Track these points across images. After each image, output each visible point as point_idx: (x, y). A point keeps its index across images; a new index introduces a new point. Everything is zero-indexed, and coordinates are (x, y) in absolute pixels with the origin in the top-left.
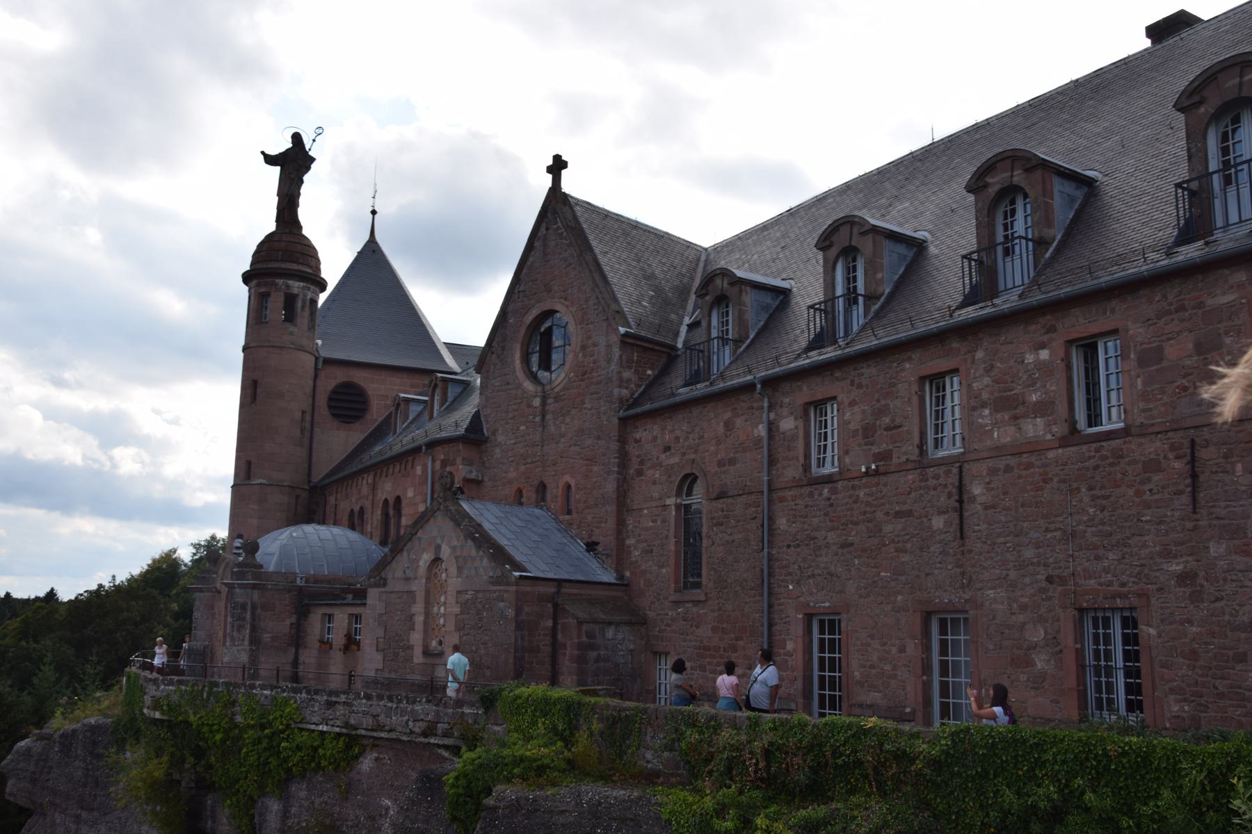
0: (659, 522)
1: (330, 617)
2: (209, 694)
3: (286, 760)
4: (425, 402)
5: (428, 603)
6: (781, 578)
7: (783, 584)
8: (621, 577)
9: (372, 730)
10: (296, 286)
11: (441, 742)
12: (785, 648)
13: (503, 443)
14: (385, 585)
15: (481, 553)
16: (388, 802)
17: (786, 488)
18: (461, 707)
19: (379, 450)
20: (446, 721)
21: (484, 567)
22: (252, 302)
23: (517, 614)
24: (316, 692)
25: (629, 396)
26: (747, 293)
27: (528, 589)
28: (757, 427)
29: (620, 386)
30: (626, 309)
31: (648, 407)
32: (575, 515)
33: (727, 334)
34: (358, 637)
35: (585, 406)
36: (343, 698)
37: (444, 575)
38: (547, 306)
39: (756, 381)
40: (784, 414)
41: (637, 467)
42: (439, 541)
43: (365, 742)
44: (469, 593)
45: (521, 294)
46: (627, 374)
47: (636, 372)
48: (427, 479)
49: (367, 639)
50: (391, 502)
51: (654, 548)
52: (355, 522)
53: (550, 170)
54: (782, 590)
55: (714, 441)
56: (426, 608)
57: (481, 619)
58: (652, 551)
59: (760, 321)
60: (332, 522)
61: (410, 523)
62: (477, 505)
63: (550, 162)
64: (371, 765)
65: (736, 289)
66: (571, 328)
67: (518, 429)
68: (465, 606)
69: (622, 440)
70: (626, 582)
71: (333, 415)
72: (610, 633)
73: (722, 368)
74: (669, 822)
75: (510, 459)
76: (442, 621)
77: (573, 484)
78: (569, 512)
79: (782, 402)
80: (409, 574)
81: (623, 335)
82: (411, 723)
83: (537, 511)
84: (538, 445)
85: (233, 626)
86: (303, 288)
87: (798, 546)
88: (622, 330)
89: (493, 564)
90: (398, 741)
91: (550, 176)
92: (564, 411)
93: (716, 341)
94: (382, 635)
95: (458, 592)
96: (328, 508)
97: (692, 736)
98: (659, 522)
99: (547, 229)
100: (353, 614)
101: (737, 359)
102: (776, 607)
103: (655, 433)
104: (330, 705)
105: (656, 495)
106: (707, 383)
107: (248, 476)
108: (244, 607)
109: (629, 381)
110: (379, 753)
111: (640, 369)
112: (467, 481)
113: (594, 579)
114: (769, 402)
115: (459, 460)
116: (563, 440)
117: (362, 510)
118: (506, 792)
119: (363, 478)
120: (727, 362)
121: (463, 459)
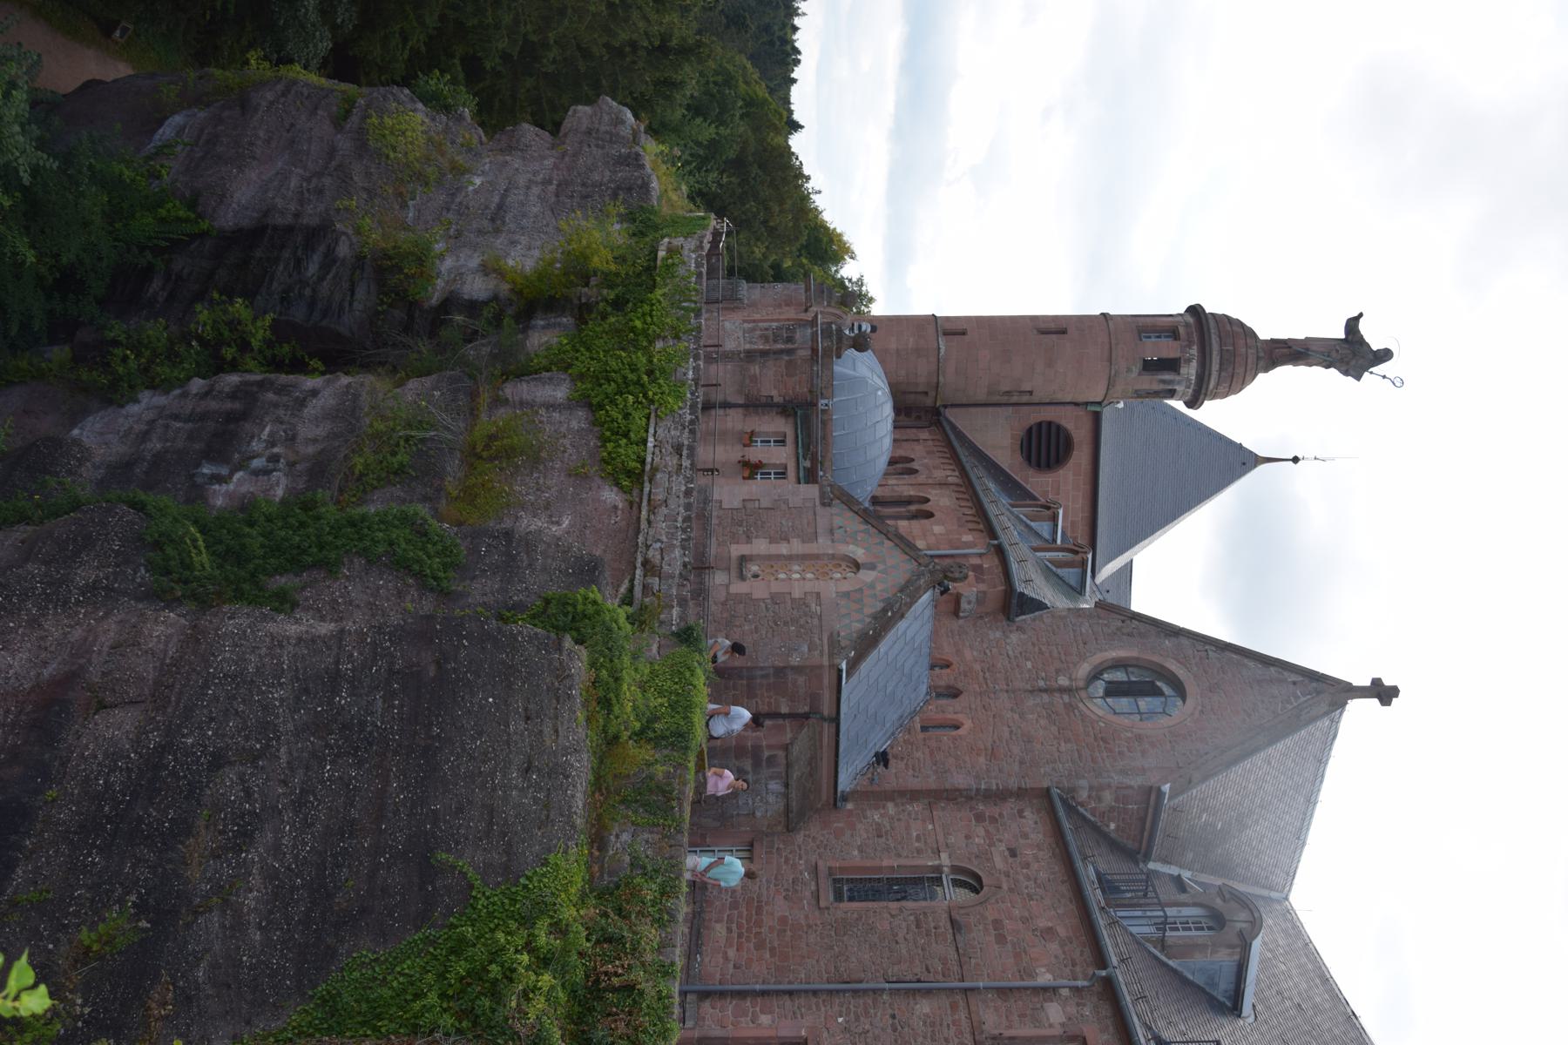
0: (917, 844)
1: (781, 442)
2: (686, 309)
3: (613, 402)
4: (1054, 540)
5: (803, 558)
6: (851, 1007)
7: (844, 1009)
8: (845, 799)
9: (649, 500)
10: (1190, 371)
11: (636, 582)
12: (762, 1012)
13: (1008, 641)
14: (823, 504)
15: (868, 620)
16: (566, 523)
17: (970, 1014)
18: (680, 604)
19: (989, 489)
20: (662, 587)
21: (851, 624)
22: (1165, 319)
23: (793, 668)
24: (692, 432)
25: (1080, 800)
26: (1231, 955)
27: (826, 681)
28: (1048, 971)
29: (1091, 788)
30: (1194, 791)
31: (1067, 825)
32: (921, 736)
33: (1172, 929)
34: (759, 476)
35: (1063, 744)
36: (686, 463)
37: (839, 575)
38: (1191, 688)
39: (1110, 970)
40: (1069, 1009)
41: (987, 814)
42: (881, 567)
43: (635, 492)
44: (818, 608)
45: (1204, 654)
46: (1108, 797)
47: (1112, 809)
48: (957, 548)
49: (757, 488)
50: (926, 507)
51: (883, 840)
52: (899, 465)
53: (1377, 682)
54: (836, 1008)
55: (1026, 914)
56: (797, 556)
57: (786, 623)
58: (880, 836)
59: (1193, 974)
60: (897, 437)
61: (901, 531)
62: (928, 612)
63: (1387, 682)
64: (609, 500)
65: (1236, 941)
66: (1164, 721)
67: (1027, 659)
68: (801, 604)
69: (1020, 793)
70: (839, 804)
71: (1030, 431)
72: (775, 786)
73: (1125, 923)
74: (545, 863)
75: (988, 651)
76: (782, 576)
77: (961, 732)
78: (924, 729)
79: (1084, 1005)
80: (838, 534)
81: (1159, 790)
82: (658, 545)
83: (924, 688)
84: (1008, 685)
85: (766, 329)
86: (1189, 380)
87: (895, 1030)
88: (1166, 788)
89: (855, 635)
90: (638, 531)
91: (1368, 683)
92: (1053, 716)
93: (1161, 913)
94: (762, 506)
95: (818, 594)
96: (914, 430)
97: (649, 891)
98: (917, 844)
99: (1294, 683)
100: (786, 468)
101: (1138, 943)
102: (814, 1000)
103: (1032, 836)
104: (678, 449)
105: (952, 839)
106: (1103, 904)
107: (946, 334)
108: (790, 340)
109: (1099, 799)
110: (622, 510)
111: (1116, 814)
112: (957, 599)
113: (841, 764)
114: (1083, 987)
115: (983, 587)
116: (1016, 716)
117: (916, 471)
118: (579, 662)
119: (954, 470)
120: (1134, 930)
121: (985, 593)
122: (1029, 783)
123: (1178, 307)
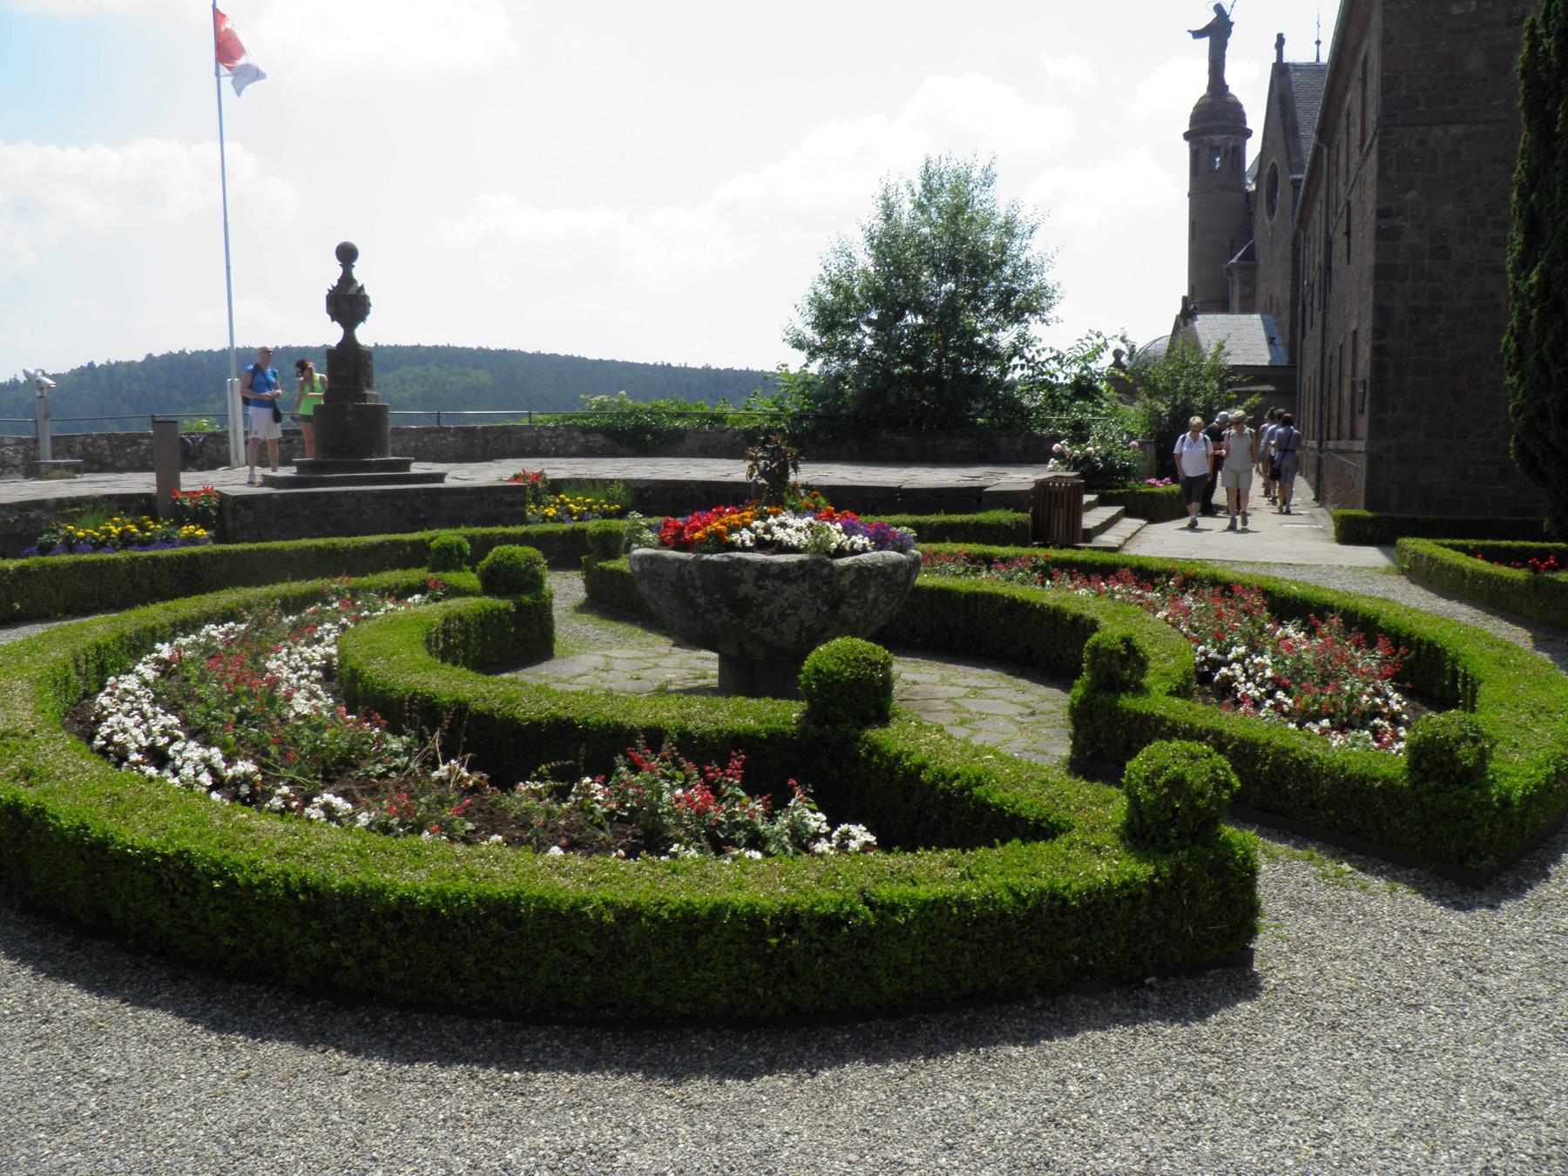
10: (1218, 139)
122: (1290, 257)
123: (1185, 148)
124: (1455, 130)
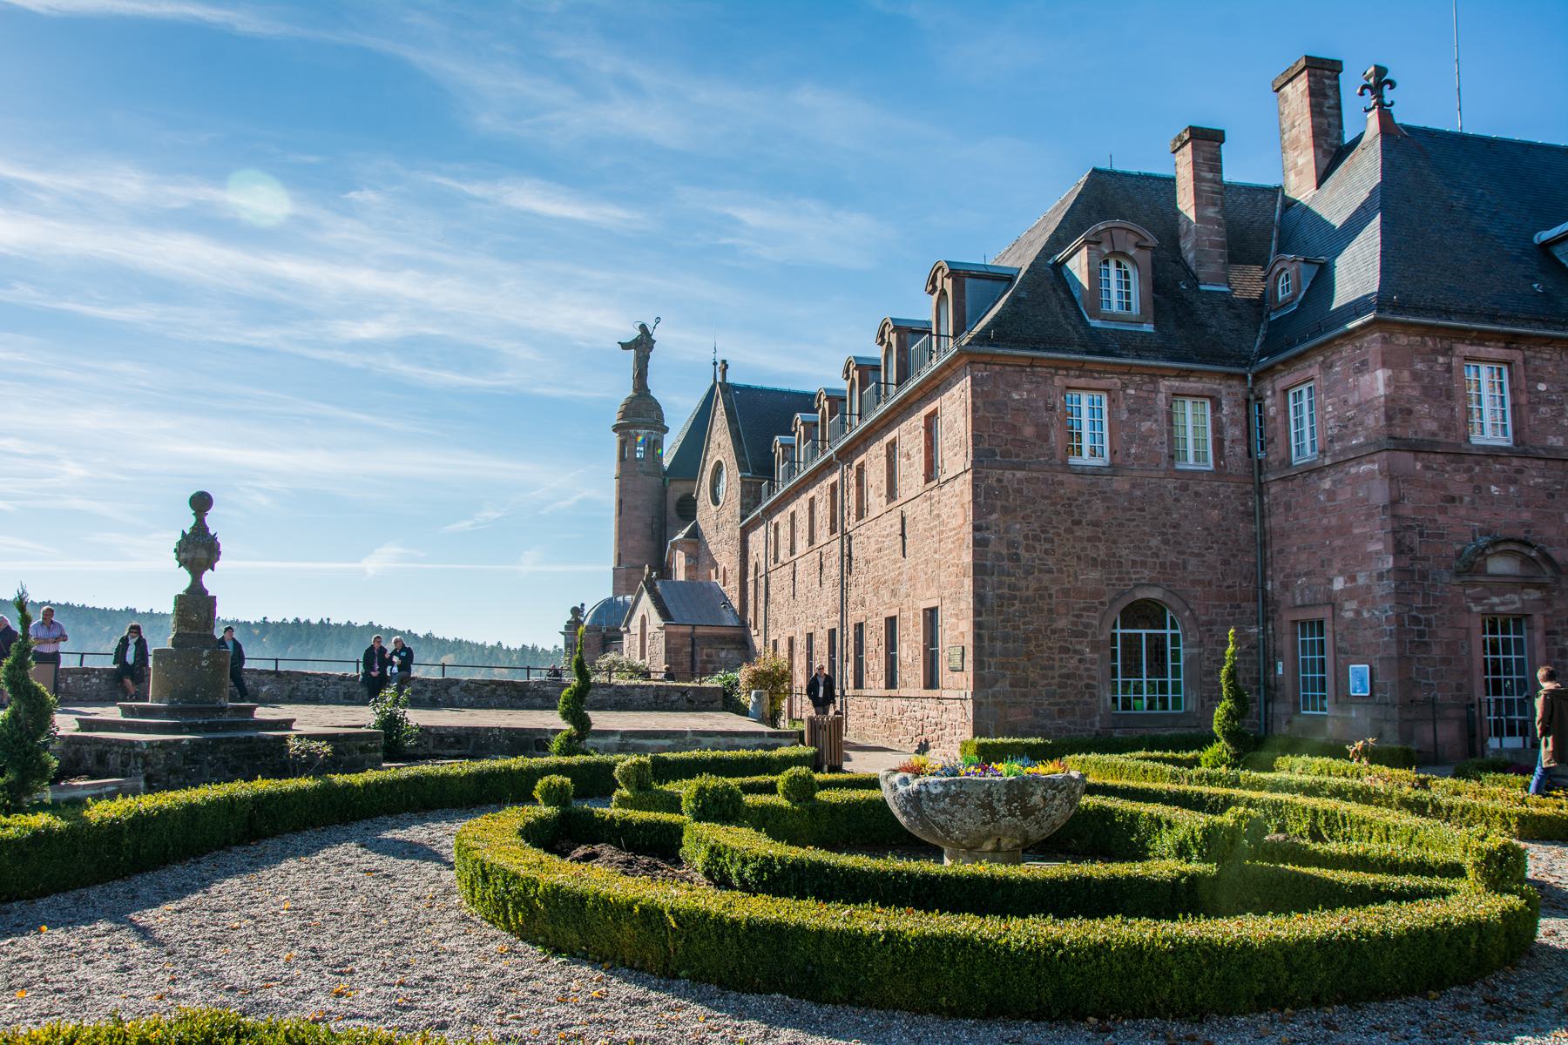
124: (1019, 474)
